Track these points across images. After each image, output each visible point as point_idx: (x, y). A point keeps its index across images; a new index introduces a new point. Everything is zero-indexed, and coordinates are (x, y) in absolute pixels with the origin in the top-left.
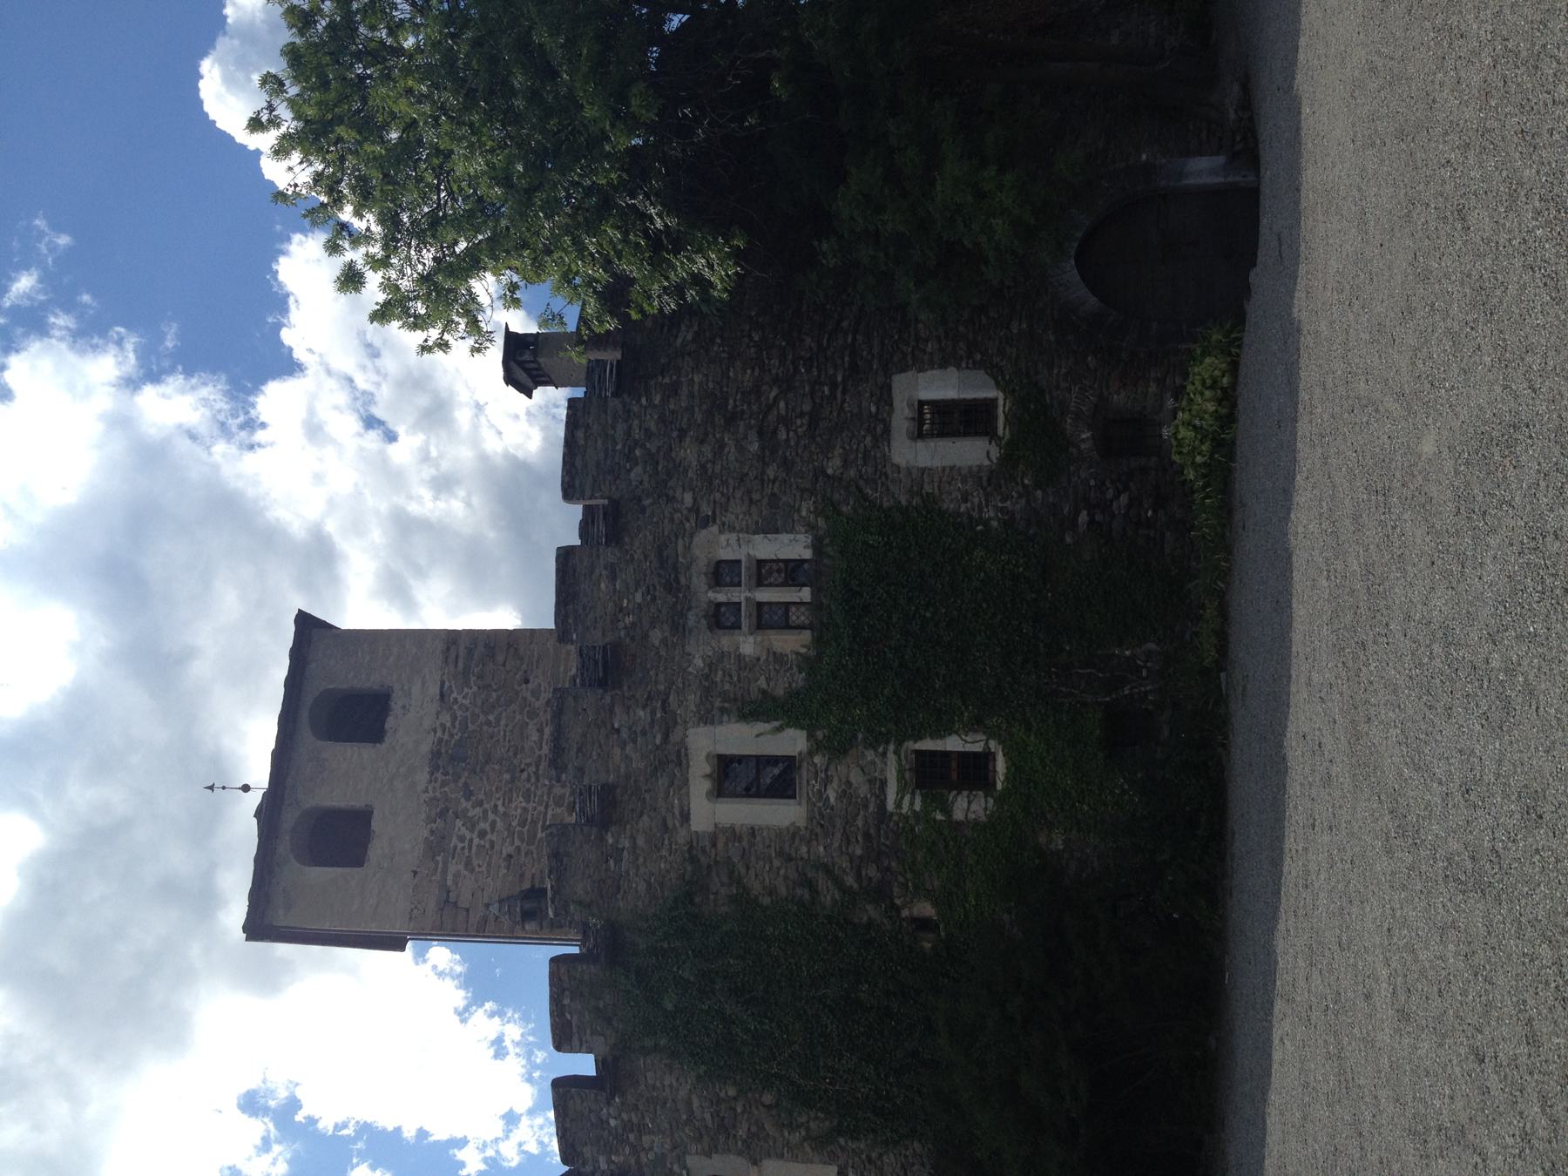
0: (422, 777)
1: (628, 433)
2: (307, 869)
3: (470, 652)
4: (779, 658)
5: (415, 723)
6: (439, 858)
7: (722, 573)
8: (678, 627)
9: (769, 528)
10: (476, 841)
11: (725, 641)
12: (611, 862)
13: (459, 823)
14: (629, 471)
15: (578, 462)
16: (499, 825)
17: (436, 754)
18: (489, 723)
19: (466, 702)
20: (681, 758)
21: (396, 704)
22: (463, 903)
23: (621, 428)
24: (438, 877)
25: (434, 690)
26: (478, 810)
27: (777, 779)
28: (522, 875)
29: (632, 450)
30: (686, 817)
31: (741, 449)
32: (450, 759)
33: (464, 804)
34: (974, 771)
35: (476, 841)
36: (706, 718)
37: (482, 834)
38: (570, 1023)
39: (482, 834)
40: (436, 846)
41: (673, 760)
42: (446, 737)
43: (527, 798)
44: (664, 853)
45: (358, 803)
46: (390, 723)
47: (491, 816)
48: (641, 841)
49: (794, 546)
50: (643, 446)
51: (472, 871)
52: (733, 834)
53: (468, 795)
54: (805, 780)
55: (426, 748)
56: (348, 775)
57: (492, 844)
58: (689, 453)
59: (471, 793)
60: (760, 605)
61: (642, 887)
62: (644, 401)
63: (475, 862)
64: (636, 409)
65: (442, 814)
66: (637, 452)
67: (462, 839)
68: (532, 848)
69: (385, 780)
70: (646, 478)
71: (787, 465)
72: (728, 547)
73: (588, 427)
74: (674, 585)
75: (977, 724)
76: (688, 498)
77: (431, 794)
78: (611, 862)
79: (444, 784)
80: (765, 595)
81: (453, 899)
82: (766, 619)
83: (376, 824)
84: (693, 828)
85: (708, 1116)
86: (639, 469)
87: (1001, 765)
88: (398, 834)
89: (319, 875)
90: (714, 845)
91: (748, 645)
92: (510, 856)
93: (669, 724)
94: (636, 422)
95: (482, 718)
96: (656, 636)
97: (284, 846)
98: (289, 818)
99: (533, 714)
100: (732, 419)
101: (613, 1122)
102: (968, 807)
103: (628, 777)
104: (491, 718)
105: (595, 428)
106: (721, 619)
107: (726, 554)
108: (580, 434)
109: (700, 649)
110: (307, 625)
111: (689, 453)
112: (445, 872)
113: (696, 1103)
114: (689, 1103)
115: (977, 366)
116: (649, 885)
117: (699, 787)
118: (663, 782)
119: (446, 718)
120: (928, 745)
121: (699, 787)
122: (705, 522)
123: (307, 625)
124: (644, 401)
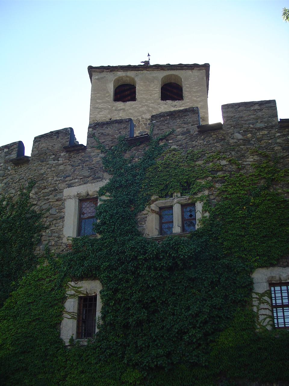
1: (260, 129)
2: (113, 82)
12: (54, 156)
14: (239, 133)
15: (241, 108)
23: (262, 125)
29: (251, 132)
30: (70, 186)
44: (55, 178)
46: (169, 102)
48: (62, 167)
50: (252, 137)
52: (61, 209)
60: (171, 207)
61: (42, 171)
62: (278, 134)
64: (273, 131)
66: (249, 135)
70: (235, 140)
73: (261, 110)
77: (141, 120)
78: (54, 156)
79: (145, 124)
80: (177, 210)
83: (129, 103)
84: (65, 190)
86: (240, 136)
90: (57, 200)
94: (266, 132)
97: (120, 74)
98: (131, 74)
103: (89, 157)
105: (260, 114)
108: (257, 107)
110: (206, 67)
116: (42, 174)
123: (206, 67)
124: (278, 134)
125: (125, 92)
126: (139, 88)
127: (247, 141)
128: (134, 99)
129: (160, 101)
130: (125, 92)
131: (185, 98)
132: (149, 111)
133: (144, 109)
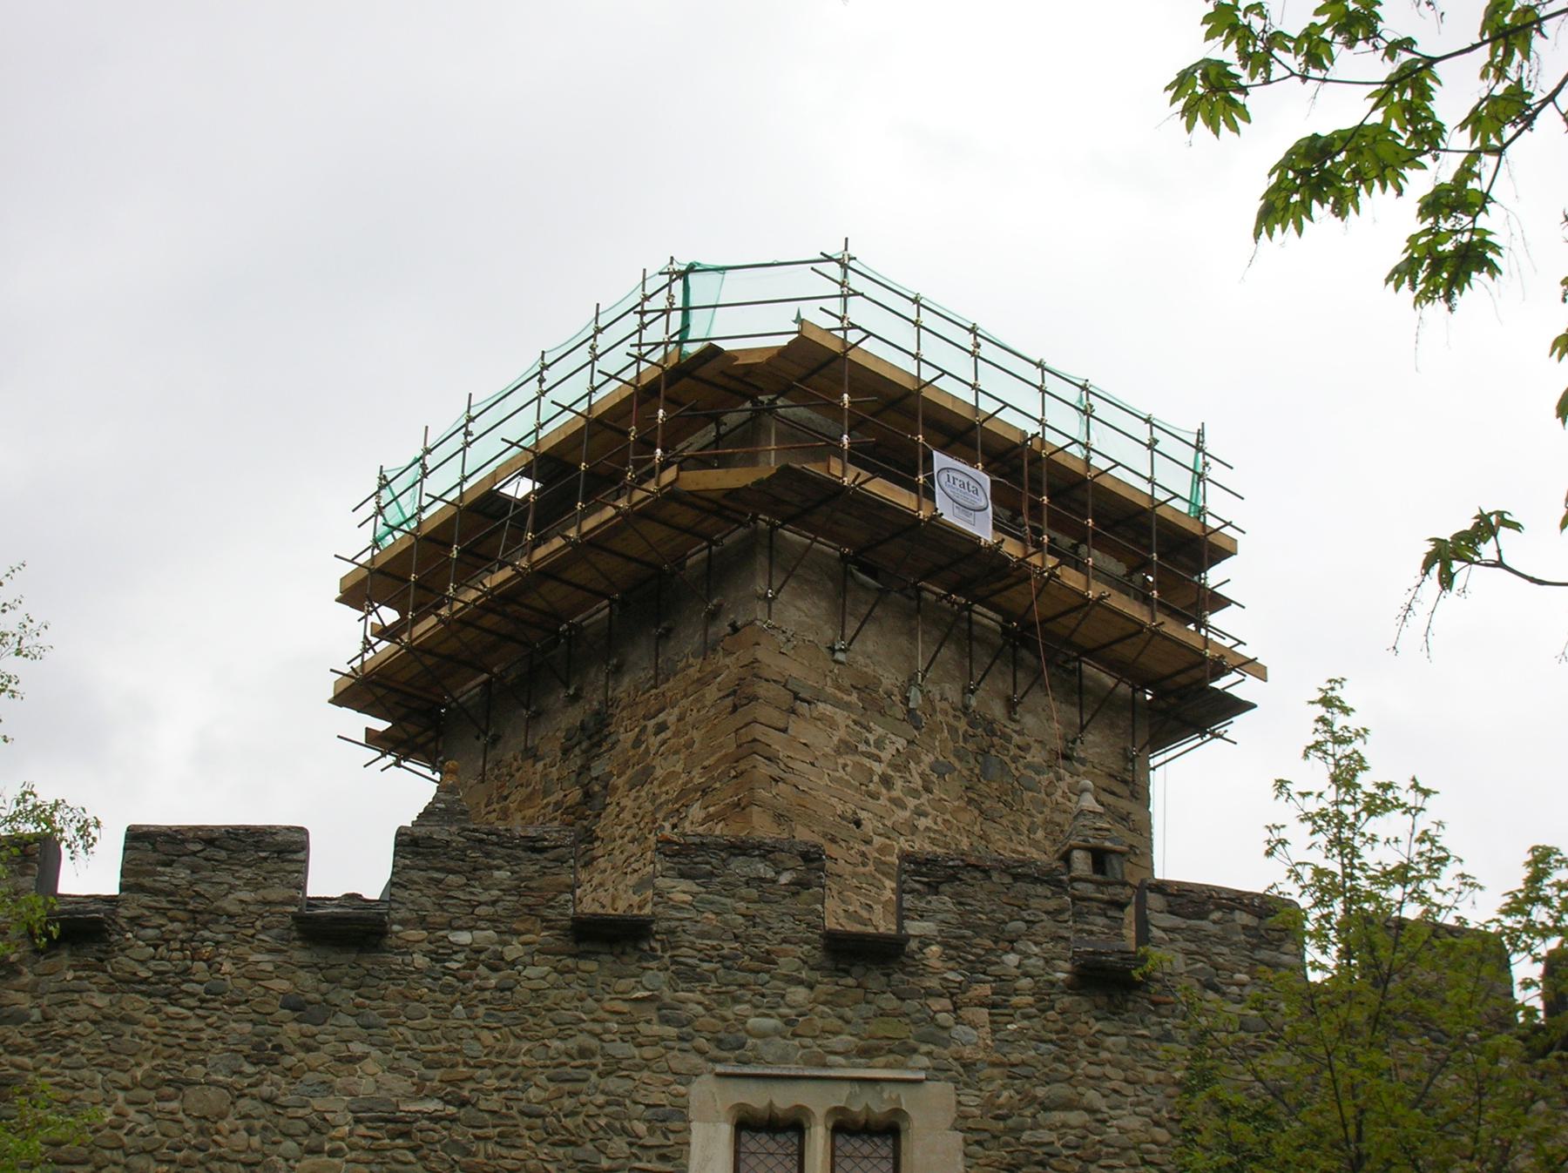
6: (854, 698)
10: (878, 768)
13: (901, 743)
16: (902, 815)
18: (1032, 829)
19: (1058, 796)
22: (796, 726)
24: (829, 690)
26: (917, 782)
28: (833, 840)
33: (928, 759)
35: (878, 768)
37: (886, 781)
38: (1202, 916)
39: (886, 781)
42: (1013, 751)
47: (912, 802)
51: (838, 751)
53: (940, 769)
57: (875, 796)
59: (941, 776)
63: (849, 759)
67: (879, 744)
68: (870, 868)
81: (803, 708)
85: (1045, 1136)
92: (858, 824)
95: (1039, 818)
101: (1012, 959)
104: (1040, 834)
112: (837, 704)
113: (1075, 1118)
114: (1068, 1106)
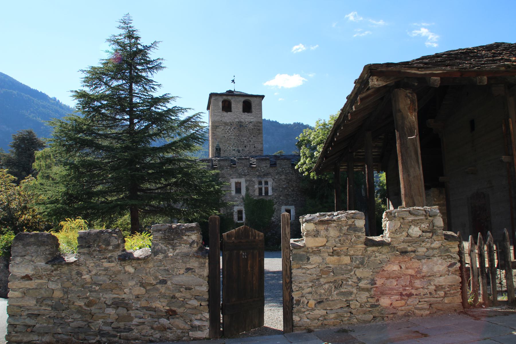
0: (237, 120)
3: (258, 126)
4: (254, 191)
5: (246, 118)
7: (266, 183)
8: (259, 176)
9: (273, 189)
11: (257, 183)
17: (241, 122)
20: (240, 177)
21: (249, 114)
23: (287, 166)
25: (252, 120)
27: (238, 190)
30: (232, 178)
31: (284, 184)
32: (240, 125)
34: (240, 218)
36: (246, 181)
40: (226, 124)
41: (240, 176)
43: (234, 139)
45: (233, 109)
46: (246, 113)
49: (270, 193)
54: (237, 195)
55: (242, 120)
56: (237, 106)
58: (283, 177)
65: (231, 124)
69: (237, 113)
71: (282, 191)
72: (270, 183)
74: (264, 175)
75: (246, 218)
76: (277, 177)
82: (260, 189)
83: (229, 113)
87: (241, 222)
88: (228, 117)
89: (220, 104)
91: (257, 186)
93: (245, 175)
96: (257, 173)
97: (225, 98)
98: (229, 98)
99: (248, 138)
100: (288, 183)
102: (236, 217)
106: (260, 183)
107: (269, 183)
109: (256, 180)
110: (263, 97)
111: (283, 177)
115: (295, 218)
117: (237, 180)
118: (237, 174)
119: (247, 123)
120: (244, 212)
121: (237, 180)
122: (273, 180)
123: (263, 97)
125: (227, 107)
126: (233, 105)
127: (282, 171)
128: (231, 111)
129: (242, 113)
130: (227, 107)
131: (253, 113)
132: (238, 118)
133: (235, 116)
